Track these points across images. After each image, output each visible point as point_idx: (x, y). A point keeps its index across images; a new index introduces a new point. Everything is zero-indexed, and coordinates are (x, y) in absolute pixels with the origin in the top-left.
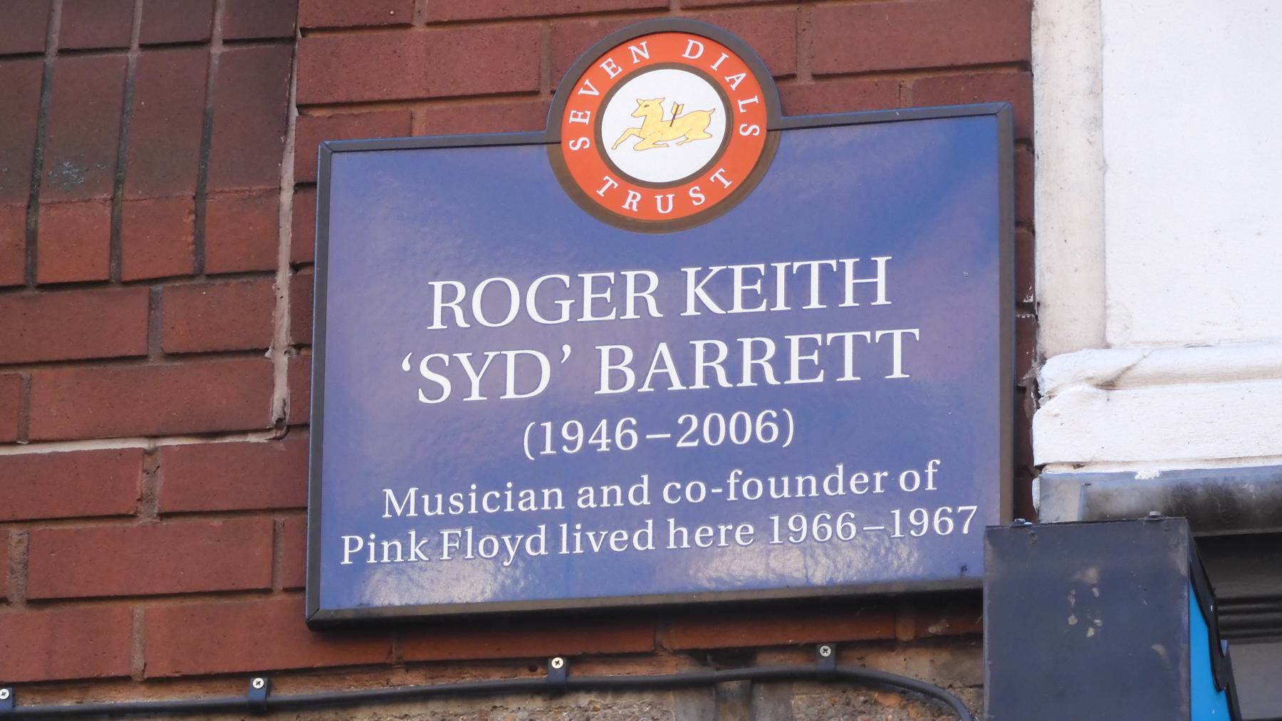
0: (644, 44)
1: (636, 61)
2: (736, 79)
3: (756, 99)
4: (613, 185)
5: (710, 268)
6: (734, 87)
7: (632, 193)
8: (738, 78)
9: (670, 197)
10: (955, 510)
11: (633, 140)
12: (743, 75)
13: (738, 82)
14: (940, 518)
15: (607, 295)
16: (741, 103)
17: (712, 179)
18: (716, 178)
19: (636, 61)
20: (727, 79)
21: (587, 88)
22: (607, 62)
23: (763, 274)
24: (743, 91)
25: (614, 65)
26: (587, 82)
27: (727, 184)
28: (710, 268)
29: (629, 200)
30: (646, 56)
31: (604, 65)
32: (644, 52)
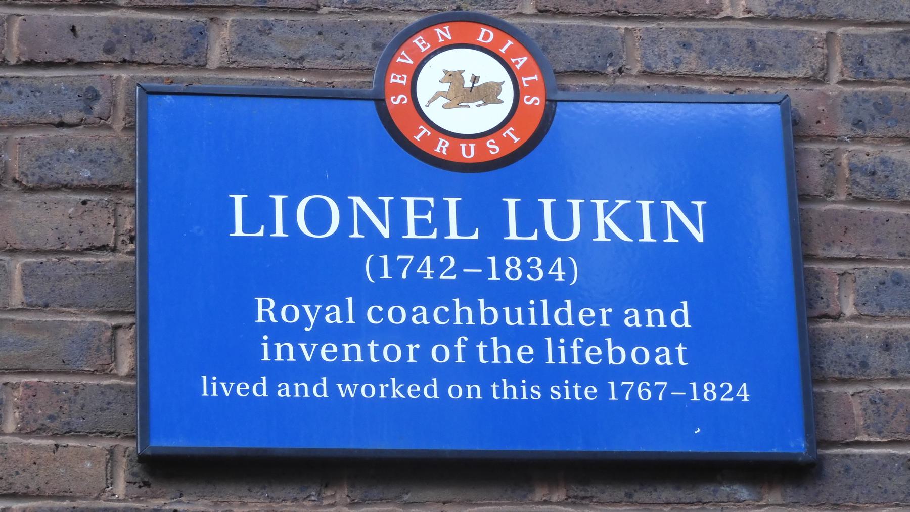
0: (446, 28)
1: (441, 40)
2: (519, 61)
3: (536, 78)
4: (426, 133)
5: (617, 201)
6: (518, 67)
7: (442, 140)
8: (521, 60)
9: (472, 146)
10: (652, 383)
11: (442, 101)
12: (525, 59)
13: (521, 63)
14: (642, 389)
15: (429, 217)
16: (524, 79)
17: (504, 135)
18: (507, 134)
19: (441, 40)
20: (513, 60)
21: (403, 57)
22: (418, 39)
23: (433, 206)
24: (526, 70)
25: (424, 42)
26: (403, 53)
27: (516, 140)
28: (617, 201)
29: (440, 145)
30: (449, 37)
31: (416, 41)
32: (440, 34)
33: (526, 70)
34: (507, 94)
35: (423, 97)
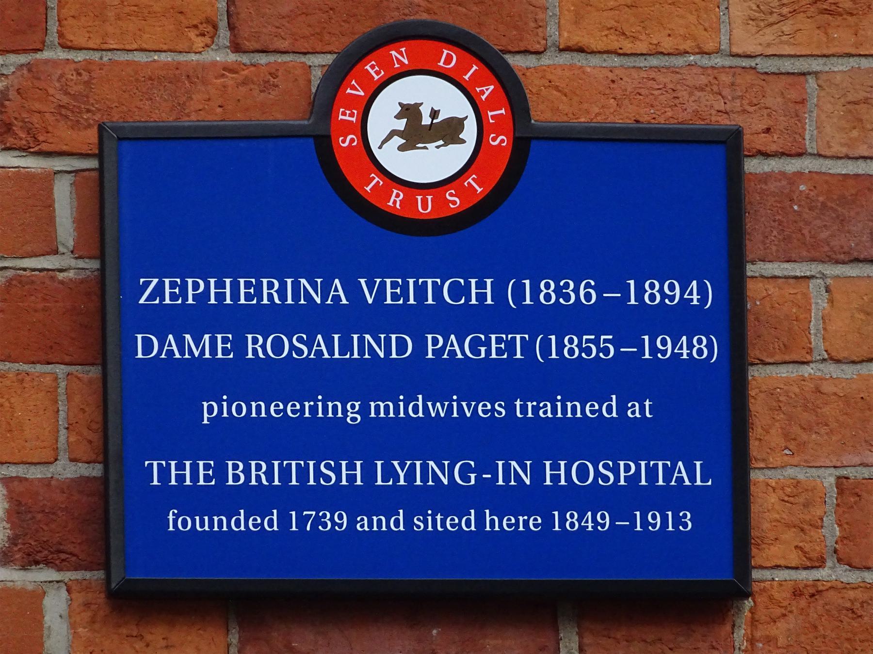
2: (485, 91)
3: (503, 111)
8: (487, 90)
13: (487, 93)
16: (490, 114)
20: (478, 89)
24: (492, 103)
25: (377, 68)
29: (393, 198)
33: (492, 103)
34: (470, 132)
35: (375, 137)
